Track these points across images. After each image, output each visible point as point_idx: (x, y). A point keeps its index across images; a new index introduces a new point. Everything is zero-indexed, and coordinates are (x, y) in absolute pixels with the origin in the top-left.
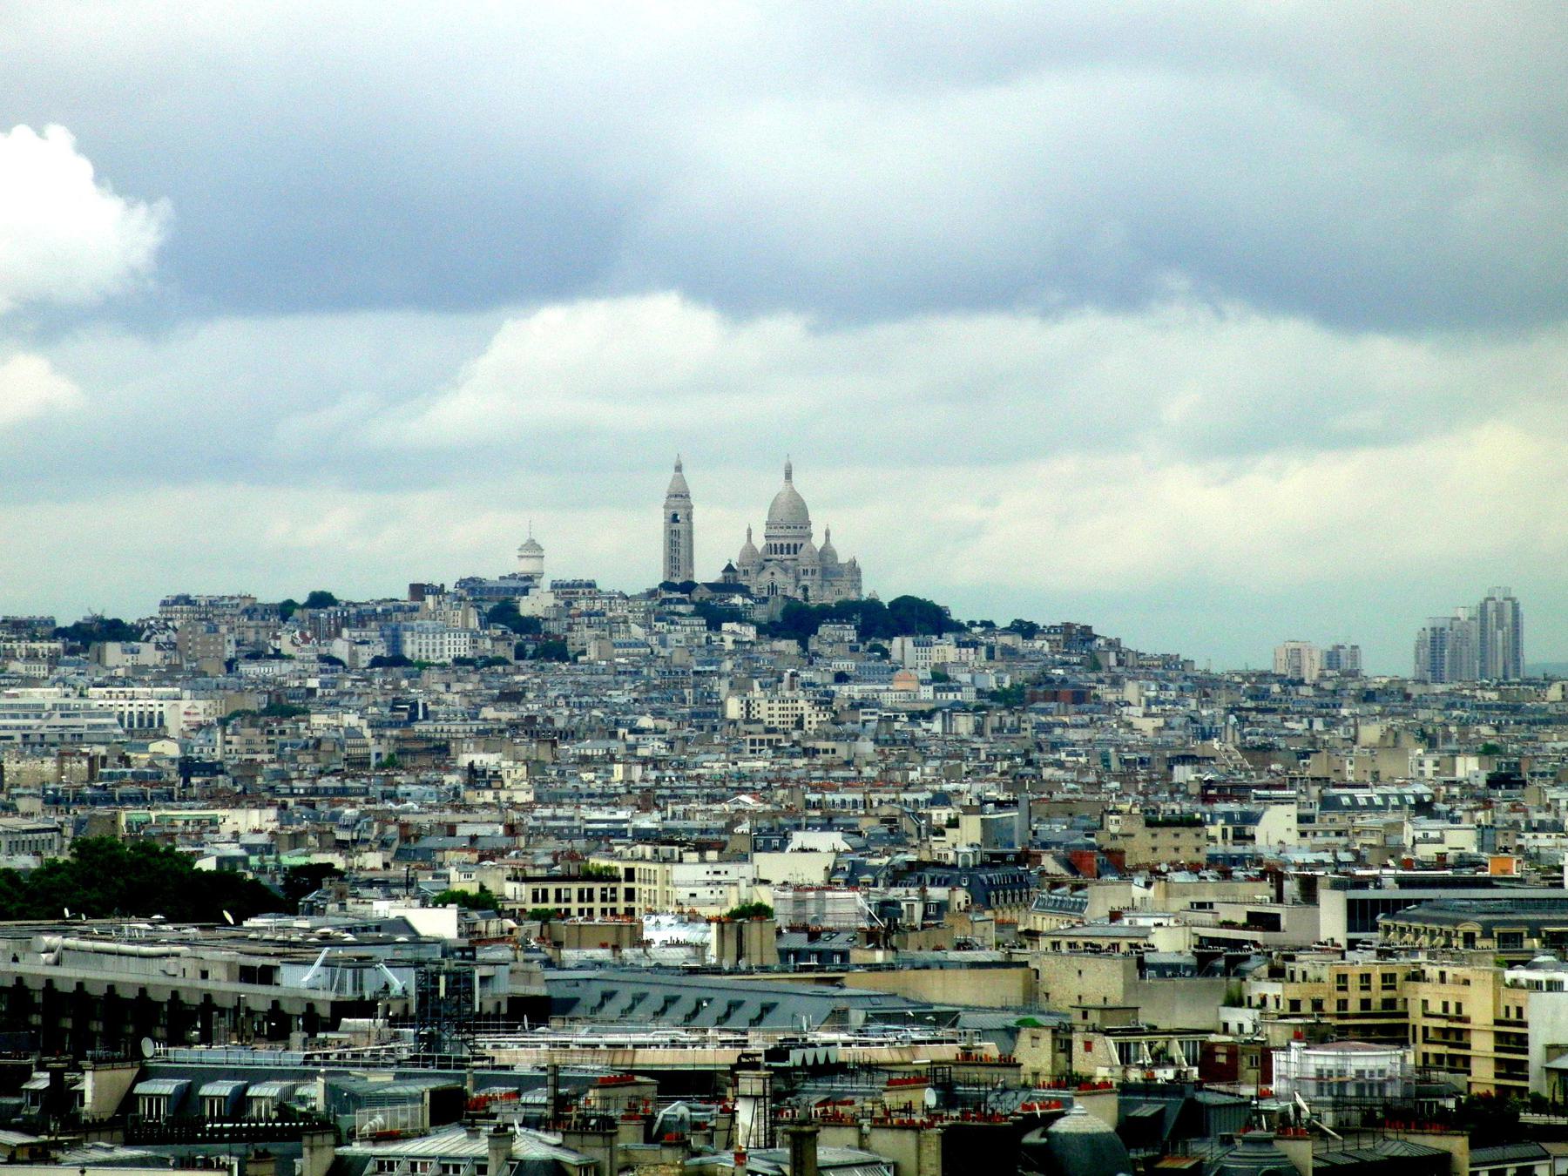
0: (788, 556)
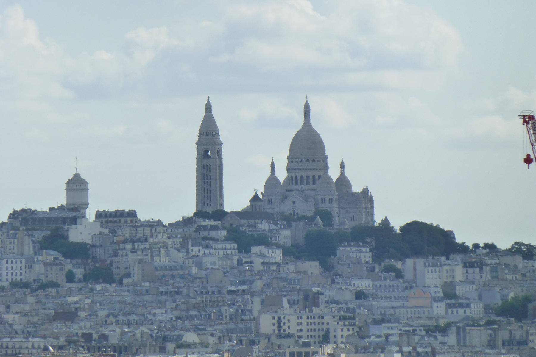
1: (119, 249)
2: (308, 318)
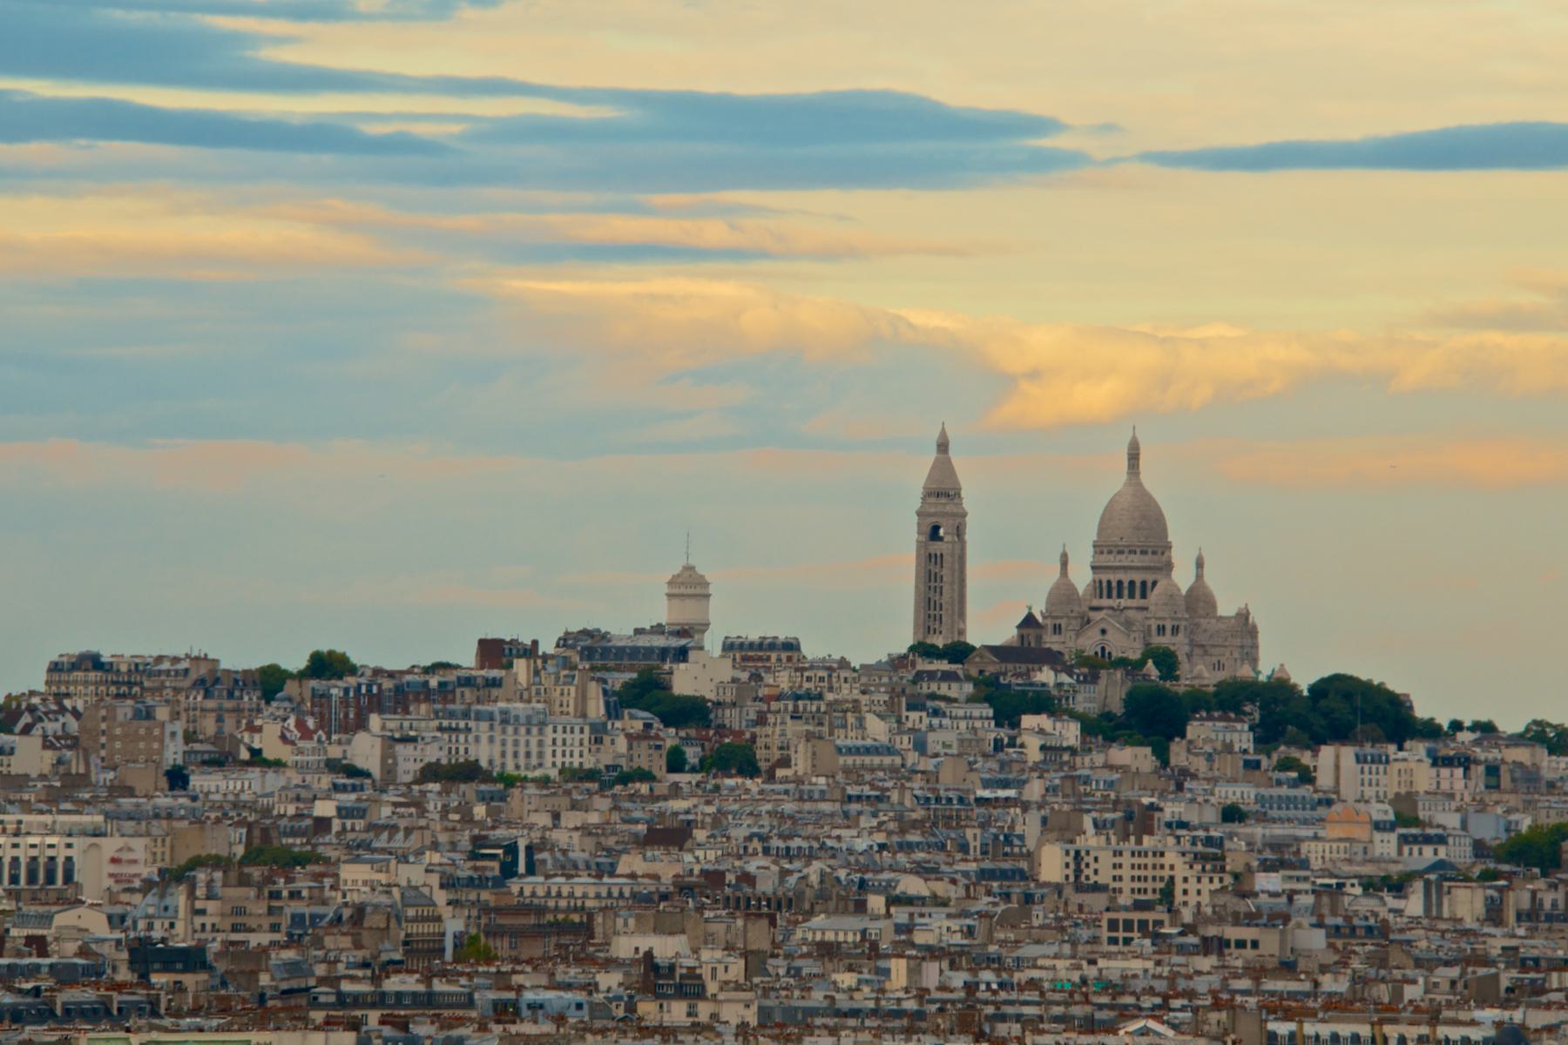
1: (769, 711)
2: (1133, 854)
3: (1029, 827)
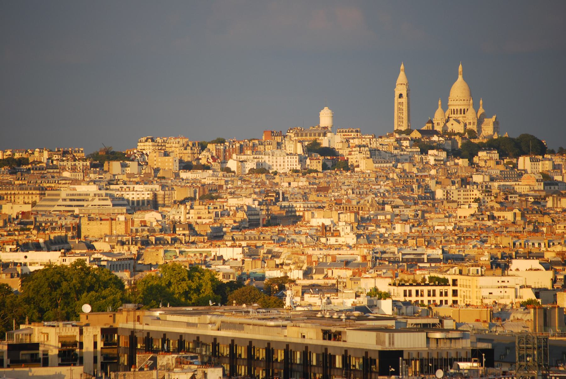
0: (460, 115)
1: (352, 151)
2: (464, 191)
3: (432, 184)
